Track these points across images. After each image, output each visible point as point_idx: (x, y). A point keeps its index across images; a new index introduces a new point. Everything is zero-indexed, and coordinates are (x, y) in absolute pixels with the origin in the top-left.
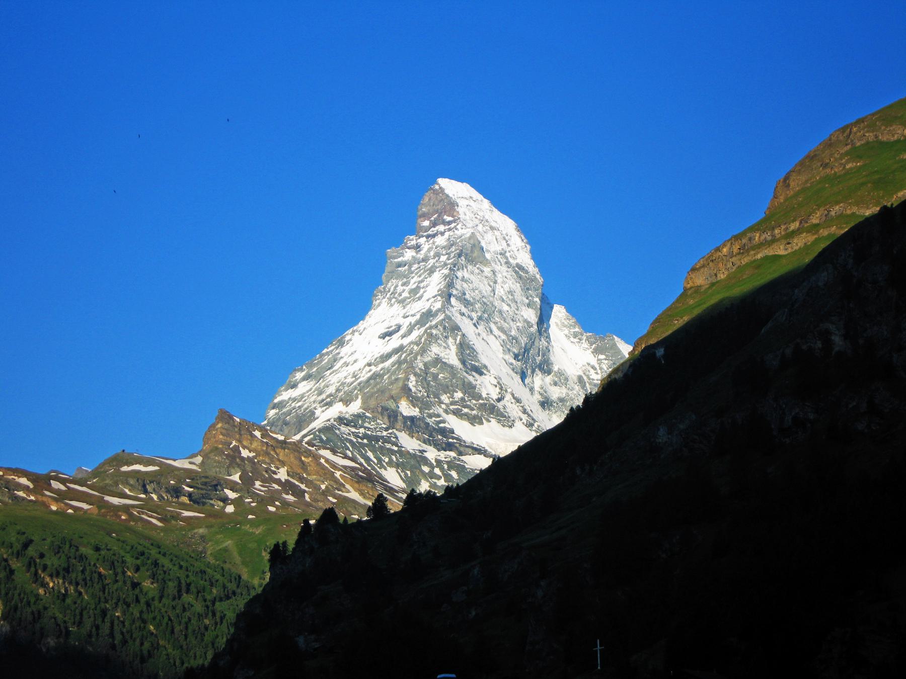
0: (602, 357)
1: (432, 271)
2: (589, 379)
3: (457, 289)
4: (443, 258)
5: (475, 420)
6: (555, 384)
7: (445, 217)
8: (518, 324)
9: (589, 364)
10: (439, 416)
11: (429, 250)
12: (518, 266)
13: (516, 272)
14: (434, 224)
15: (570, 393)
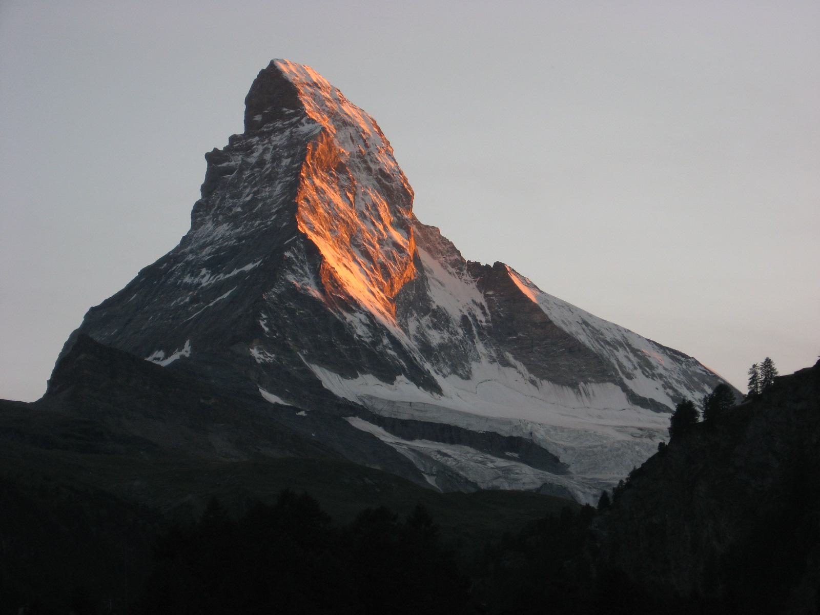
0: (491, 293)
1: (270, 179)
2: (476, 320)
3: (308, 201)
4: (286, 162)
5: (348, 370)
6: (435, 327)
7: (285, 109)
8: (387, 248)
9: (474, 302)
10: (302, 364)
11: (266, 150)
12: (380, 170)
13: (379, 181)
14: (268, 119)
15: (453, 338)
